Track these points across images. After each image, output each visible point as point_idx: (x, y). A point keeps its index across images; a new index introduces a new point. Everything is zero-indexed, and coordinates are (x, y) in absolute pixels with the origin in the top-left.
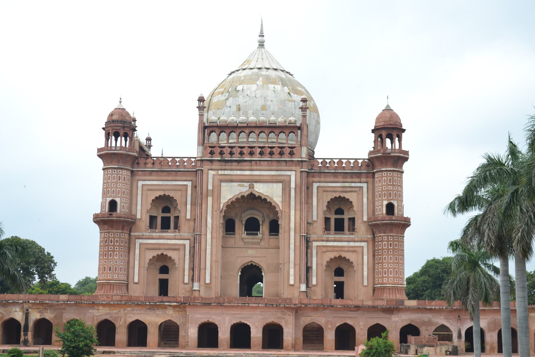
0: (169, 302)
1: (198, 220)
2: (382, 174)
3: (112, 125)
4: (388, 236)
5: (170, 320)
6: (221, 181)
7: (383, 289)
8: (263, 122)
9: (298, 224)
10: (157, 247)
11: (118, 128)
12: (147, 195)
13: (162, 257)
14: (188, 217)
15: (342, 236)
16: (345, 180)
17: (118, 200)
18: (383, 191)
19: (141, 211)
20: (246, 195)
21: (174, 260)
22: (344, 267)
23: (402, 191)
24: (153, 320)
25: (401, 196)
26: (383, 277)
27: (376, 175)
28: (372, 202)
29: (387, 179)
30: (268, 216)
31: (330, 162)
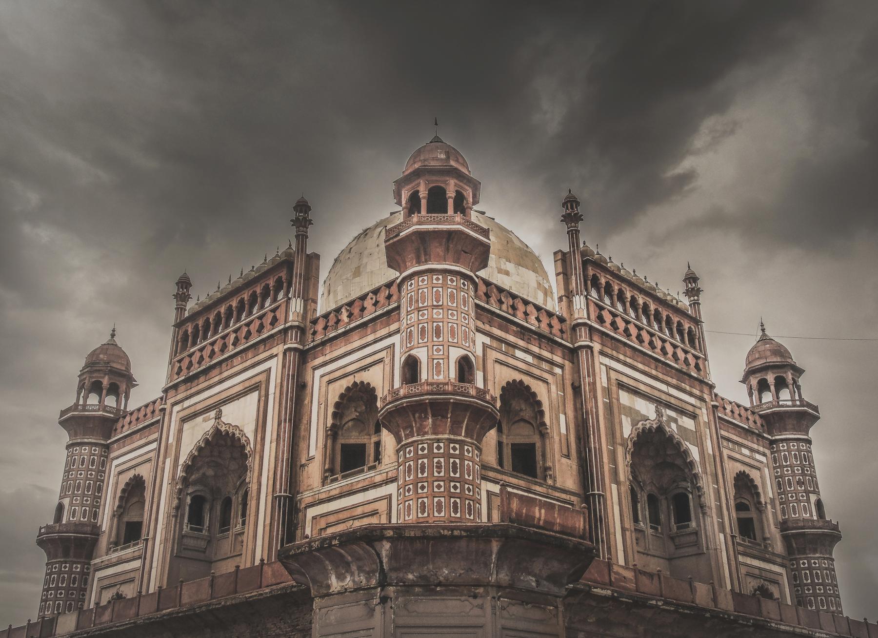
6: (184, 420)
12: (117, 483)
17: (66, 502)
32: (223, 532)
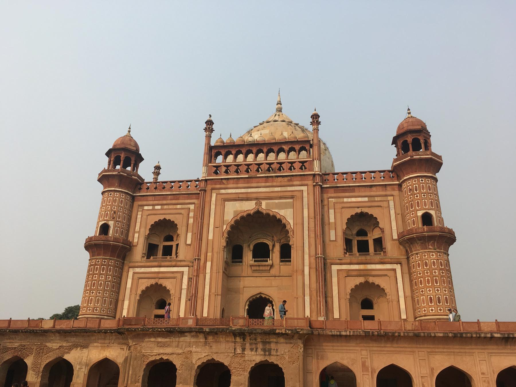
14: (189, 242)
15: (368, 257)
17: (111, 223)
20: (252, 212)
21: (169, 291)
27: (404, 186)
30: (279, 241)
32: (233, 262)
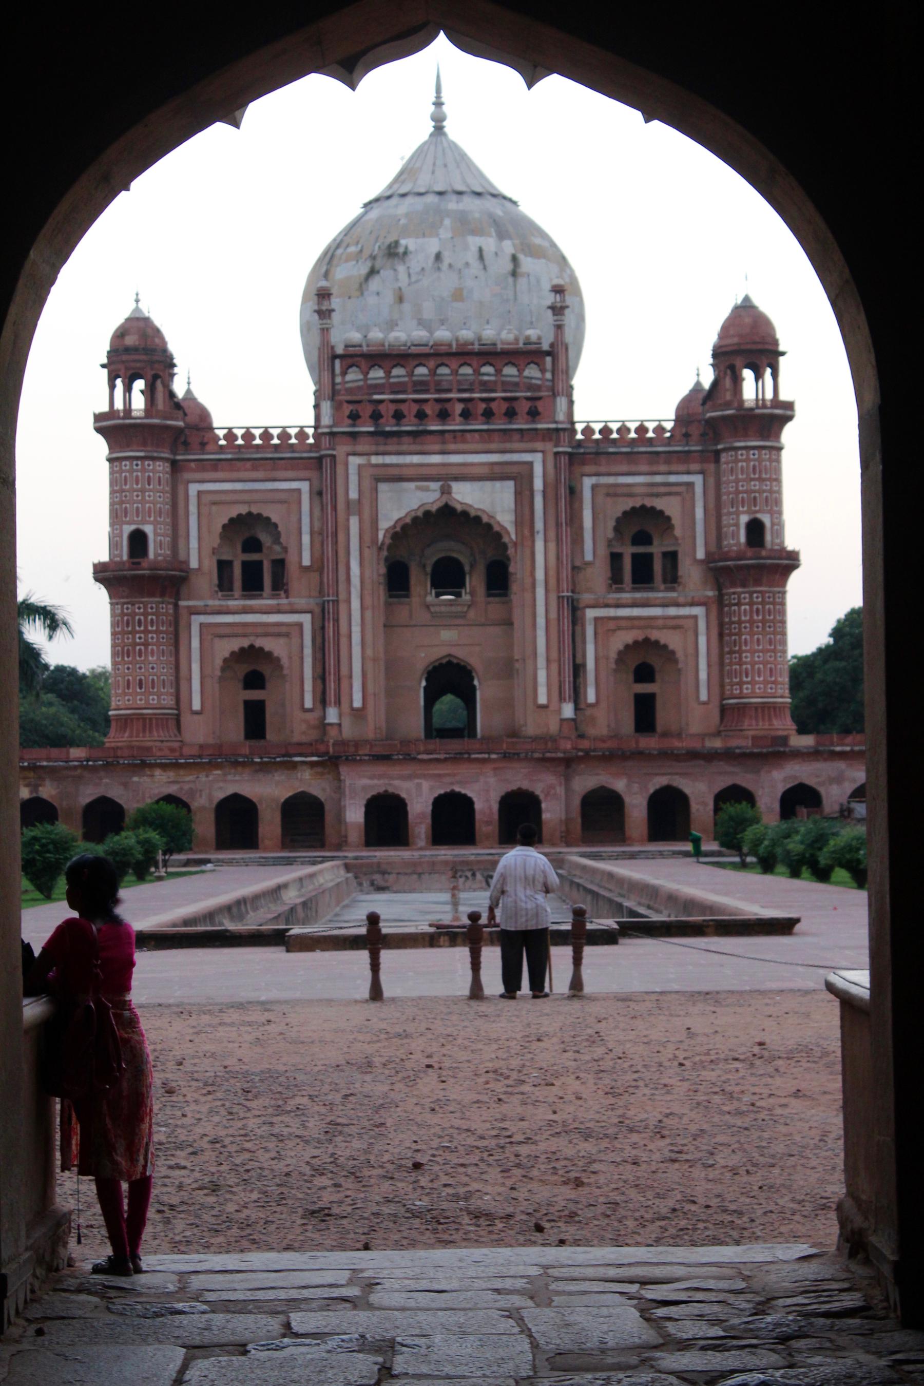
0: (300, 755)
1: (328, 567)
2: (736, 455)
3: (125, 358)
4: (751, 594)
5: (303, 793)
6: (378, 479)
7: (742, 709)
8: (466, 344)
9: (552, 573)
10: (240, 631)
11: (138, 365)
13: (251, 654)
14: (306, 561)
15: (651, 595)
16: (655, 468)
17: (148, 529)
18: (737, 492)
19: (197, 553)
20: (434, 508)
21: (278, 659)
22: (655, 661)
23: (779, 492)
24: (269, 791)
25: (778, 502)
26: (741, 684)
27: (724, 457)
28: (716, 514)
29: (748, 466)
31: (619, 431)
